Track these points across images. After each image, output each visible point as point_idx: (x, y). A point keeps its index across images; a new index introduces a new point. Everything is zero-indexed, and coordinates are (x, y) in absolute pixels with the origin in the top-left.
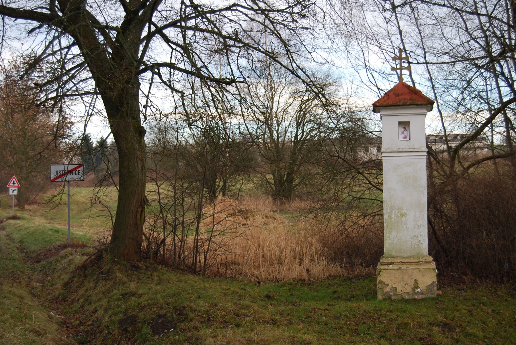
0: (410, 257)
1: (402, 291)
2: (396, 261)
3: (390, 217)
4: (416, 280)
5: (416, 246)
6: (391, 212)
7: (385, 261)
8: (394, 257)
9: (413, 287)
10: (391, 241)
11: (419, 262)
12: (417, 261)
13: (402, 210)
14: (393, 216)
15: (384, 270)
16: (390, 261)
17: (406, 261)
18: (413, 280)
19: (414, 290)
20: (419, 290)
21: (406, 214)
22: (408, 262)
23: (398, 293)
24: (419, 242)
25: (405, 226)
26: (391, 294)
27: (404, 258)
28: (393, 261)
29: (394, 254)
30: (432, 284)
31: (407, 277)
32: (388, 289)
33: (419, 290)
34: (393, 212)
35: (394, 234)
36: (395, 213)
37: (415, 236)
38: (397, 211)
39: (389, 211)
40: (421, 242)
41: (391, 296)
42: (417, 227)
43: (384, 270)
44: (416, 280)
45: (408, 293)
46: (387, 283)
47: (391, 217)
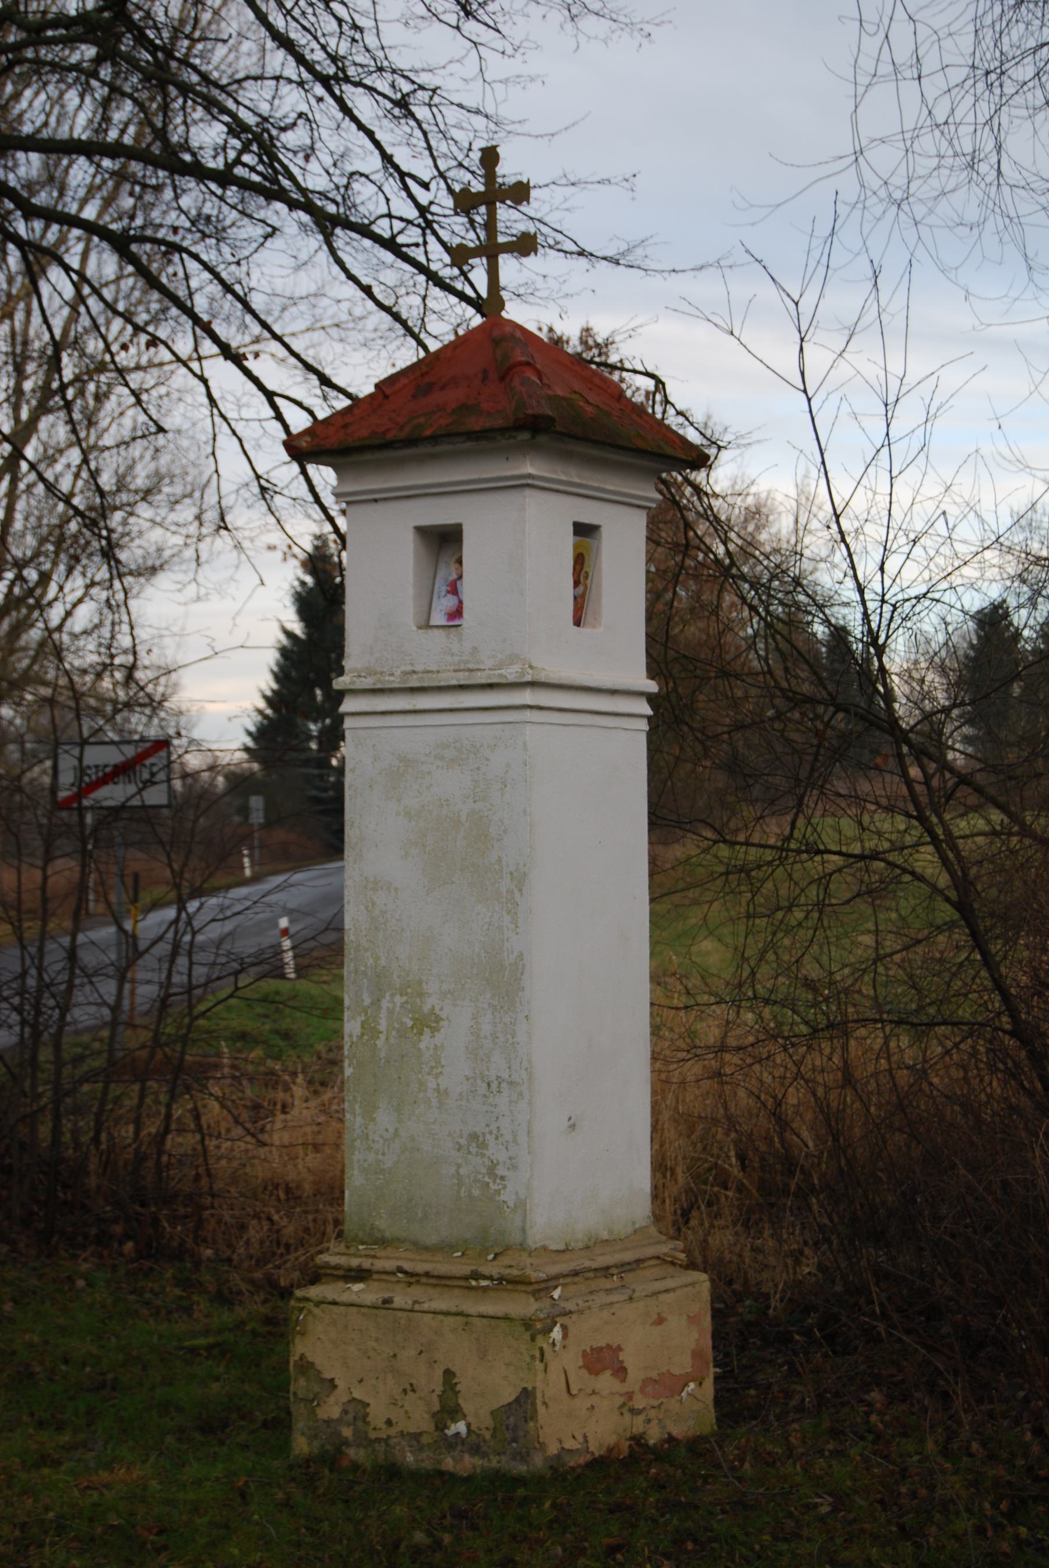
0: (444, 1248)
1: (389, 1422)
2: (379, 1265)
3: (370, 1030)
4: (449, 1374)
5: (476, 1192)
6: (376, 1002)
7: (342, 1260)
8: (384, 1242)
9: (436, 1407)
10: (371, 1157)
11: (476, 1276)
12: (466, 1270)
13: (421, 994)
14: (383, 1025)
15: (318, 1304)
16: (355, 1262)
17: (420, 1268)
18: (439, 1373)
19: (441, 1427)
20: (461, 1427)
21: (438, 1019)
22: (427, 1274)
23: (373, 1435)
24: (491, 1171)
25: (431, 1084)
26: (347, 1432)
27: (426, 1248)
28: (366, 1264)
29: (383, 1224)
30: (517, 1400)
31: (413, 1353)
32: (331, 1409)
33: (461, 1427)
34: (385, 1004)
35: (384, 1118)
36: (390, 1012)
37: (474, 1137)
38: (399, 1000)
39: (367, 1001)
40: (500, 1171)
41: (346, 1443)
42: (482, 1088)
43: (318, 1304)
44: (449, 1374)
45: (417, 1436)
46: (327, 1375)
47: (375, 1033)
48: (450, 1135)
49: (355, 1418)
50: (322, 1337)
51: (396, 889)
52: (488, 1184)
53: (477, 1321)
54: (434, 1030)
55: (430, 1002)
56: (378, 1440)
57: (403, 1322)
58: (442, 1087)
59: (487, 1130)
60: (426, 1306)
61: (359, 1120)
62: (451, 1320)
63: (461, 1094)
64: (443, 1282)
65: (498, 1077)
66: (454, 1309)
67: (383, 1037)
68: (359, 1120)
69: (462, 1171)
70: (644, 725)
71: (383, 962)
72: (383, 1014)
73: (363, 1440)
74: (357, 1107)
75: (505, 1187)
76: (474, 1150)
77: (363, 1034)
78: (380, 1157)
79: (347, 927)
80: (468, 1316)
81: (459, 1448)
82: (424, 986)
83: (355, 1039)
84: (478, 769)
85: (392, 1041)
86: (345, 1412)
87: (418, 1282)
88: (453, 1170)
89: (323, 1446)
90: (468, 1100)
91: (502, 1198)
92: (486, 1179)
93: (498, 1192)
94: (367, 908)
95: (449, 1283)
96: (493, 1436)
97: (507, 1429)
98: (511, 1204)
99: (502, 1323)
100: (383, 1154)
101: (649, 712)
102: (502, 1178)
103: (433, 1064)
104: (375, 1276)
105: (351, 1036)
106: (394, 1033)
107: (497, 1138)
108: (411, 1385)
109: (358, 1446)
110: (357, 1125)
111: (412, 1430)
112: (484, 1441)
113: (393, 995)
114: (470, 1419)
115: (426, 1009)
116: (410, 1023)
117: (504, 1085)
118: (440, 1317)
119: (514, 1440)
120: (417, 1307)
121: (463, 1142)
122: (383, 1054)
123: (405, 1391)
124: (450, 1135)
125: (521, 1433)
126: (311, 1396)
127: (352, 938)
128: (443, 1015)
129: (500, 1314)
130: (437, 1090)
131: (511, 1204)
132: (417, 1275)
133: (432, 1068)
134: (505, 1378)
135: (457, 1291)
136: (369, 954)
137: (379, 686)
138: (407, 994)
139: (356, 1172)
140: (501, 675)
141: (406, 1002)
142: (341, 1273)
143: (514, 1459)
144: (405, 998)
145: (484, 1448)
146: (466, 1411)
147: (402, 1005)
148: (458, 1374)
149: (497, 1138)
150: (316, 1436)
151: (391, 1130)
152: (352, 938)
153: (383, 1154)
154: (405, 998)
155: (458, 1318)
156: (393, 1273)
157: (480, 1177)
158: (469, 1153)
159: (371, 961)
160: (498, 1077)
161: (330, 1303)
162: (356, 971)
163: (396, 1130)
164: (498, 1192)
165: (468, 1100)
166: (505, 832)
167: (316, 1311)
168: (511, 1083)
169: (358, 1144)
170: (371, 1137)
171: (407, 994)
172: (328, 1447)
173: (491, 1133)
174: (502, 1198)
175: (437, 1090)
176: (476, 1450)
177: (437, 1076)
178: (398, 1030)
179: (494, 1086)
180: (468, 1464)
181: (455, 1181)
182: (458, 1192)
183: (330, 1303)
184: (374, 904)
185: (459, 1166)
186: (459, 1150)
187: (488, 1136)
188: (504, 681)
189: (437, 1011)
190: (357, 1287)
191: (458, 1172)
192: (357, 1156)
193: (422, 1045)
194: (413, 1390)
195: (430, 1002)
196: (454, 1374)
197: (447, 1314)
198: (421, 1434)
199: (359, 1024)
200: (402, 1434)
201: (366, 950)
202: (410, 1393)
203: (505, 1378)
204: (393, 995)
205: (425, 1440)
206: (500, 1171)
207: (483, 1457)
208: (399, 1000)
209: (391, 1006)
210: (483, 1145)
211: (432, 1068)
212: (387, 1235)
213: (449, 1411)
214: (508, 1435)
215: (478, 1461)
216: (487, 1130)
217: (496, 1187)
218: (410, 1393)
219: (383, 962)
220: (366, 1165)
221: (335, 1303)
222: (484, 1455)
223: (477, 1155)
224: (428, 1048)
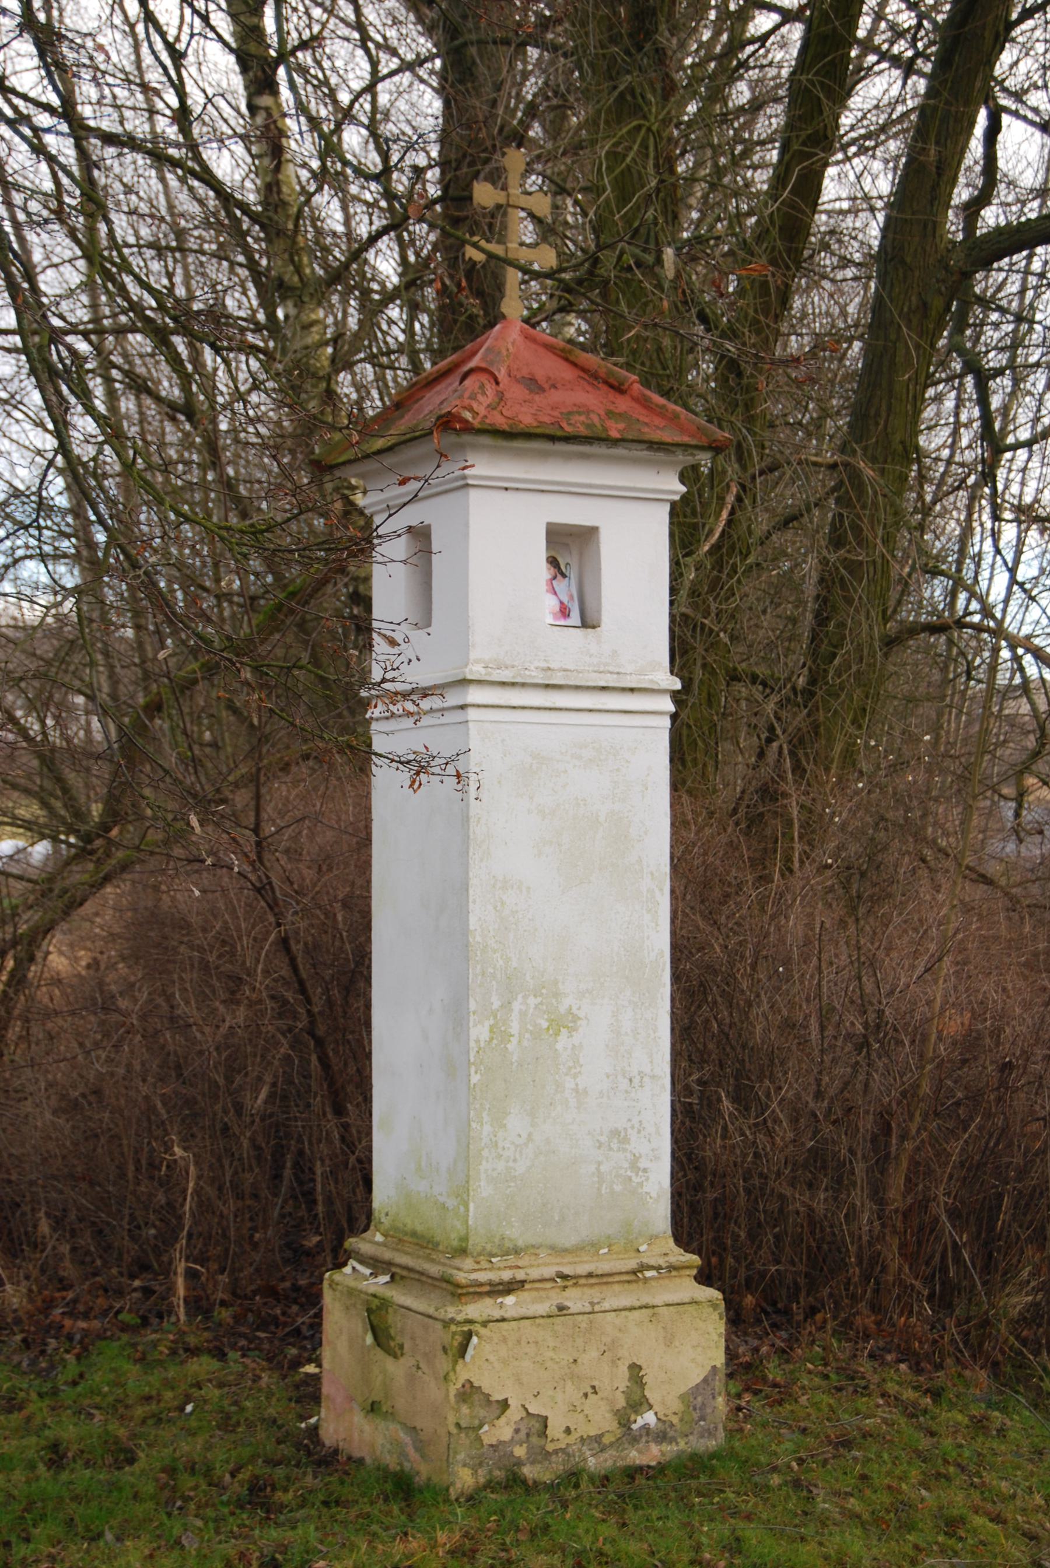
0: (592, 1247)
1: (568, 1431)
2: (535, 1273)
3: (499, 1034)
4: (635, 1369)
5: (618, 1188)
6: (507, 1005)
8: (517, 1251)
9: (621, 1402)
10: (501, 1166)
11: (643, 1267)
12: (632, 1264)
13: (557, 995)
14: (515, 1027)
15: (485, 1324)
16: (506, 1275)
17: (582, 1269)
18: (623, 1371)
19: (625, 1423)
20: (649, 1418)
21: (576, 1018)
22: (590, 1275)
23: (550, 1447)
24: (634, 1165)
25: (569, 1083)
26: (520, 1451)
27: (566, 1251)
28: (520, 1275)
29: (516, 1233)
30: (705, 1380)
31: (594, 1354)
32: (502, 1431)
33: (649, 1418)
34: (516, 1006)
35: (516, 1123)
36: (523, 1014)
37: (615, 1133)
38: (532, 1001)
39: (496, 1004)
40: (642, 1164)
41: (519, 1463)
42: (624, 1084)
43: (485, 1324)
44: (635, 1369)
45: (598, 1438)
46: (497, 1396)
47: (506, 1037)
48: (589, 1133)
49: (528, 1435)
50: (492, 1358)
51: (528, 888)
52: (630, 1179)
53: (664, 1310)
54: (572, 1030)
55: (567, 1002)
56: (556, 1452)
57: (583, 1325)
58: (580, 1087)
59: (629, 1124)
60: (606, 1305)
61: (487, 1129)
62: (636, 1314)
63: (601, 1092)
64: (605, 1280)
65: (640, 1073)
66: (638, 1304)
67: (514, 1041)
68: (487, 1129)
69: (602, 1168)
70: (667, 722)
71: (514, 964)
72: (515, 1016)
73: (543, 1455)
74: (485, 1114)
75: (647, 1179)
76: (615, 1146)
77: (492, 1039)
78: (511, 1164)
79: (472, 927)
80: (654, 1307)
81: (644, 1439)
82: (560, 986)
83: (482, 1044)
84: (618, 770)
85: (525, 1043)
86: (517, 1431)
87: (575, 1284)
88: (593, 1168)
89: (490, 1472)
90: (609, 1098)
91: (645, 1189)
92: (629, 1173)
93: (641, 1184)
94: (495, 908)
95: (610, 1279)
96: (681, 1420)
97: (695, 1409)
98: (654, 1194)
99: (690, 1308)
100: (515, 1161)
101: (672, 708)
102: (645, 1170)
103: (571, 1064)
104: (527, 1286)
105: (477, 1041)
106: (527, 1035)
107: (639, 1132)
108: (593, 1387)
109: (533, 1463)
110: (485, 1133)
111: (593, 1433)
112: (672, 1425)
113: (525, 997)
114: (656, 1408)
115: (562, 1009)
116: (545, 1025)
117: (646, 1079)
118: (623, 1313)
119: (702, 1418)
120: (597, 1308)
121: (603, 1139)
122: (515, 1058)
123: (586, 1395)
124: (589, 1133)
125: (709, 1410)
126: (476, 1422)
127: (478, 939)
128: (581, 1014)
129: (687, 1300)
130: (576, 1090)
131: (654, 1194)
132: (580, 1277)
133: (570, 1068)
134: (693, 1360)
135: (616, 1287)
136: (498, 955)
137: (519, 680)
138: (541, 995)
139: (482, 1183)
140: (652, 681)
141: (541, 1003)
142: (487, 1288)
143: (702, 1437)
144: (539, 999)
145: (671, 1433)
146: (651, 1401)
147: (536, 1007)
148: (644, 1366)
149: (639, 1132)
150: (481, 1464)
151: (524, 1135)
152: (478, 939)
153: (515, 1161)
154: (539, 999)
155: (644, 1311)
156: (553, 1280)
157: (622, 1172)
158: (611, 1149)
159: (501, 962)
160: (640, 1073)
161: (497, 1321)
162: (483, 974)
163: (530, 1135)
164: (641, 1184)
165: (609, 1098)
166: (646, 833)
167: (483, 1331)
168: (653, 1077)
169: (485, 1153)
170: (501, 1144)
171: (541, 995)
172: (497, 1473)
173: (633, 1127)
174: (645, 1189)
175: (576, 1090)
176: (662, 1437)
177: (575, 1076)
178: (531, 1033)
179: (636, 1081)
180: (653, 1454)
181: (596, 1179)
182: (599, 1189)
183: (497, 1321)
184: (503, 903)
185: (599, 1163)
186: (599, 1147)
187: (630, 1131)
188: (656, 687)
189: (574, 1010)
190: (510, 1300)
191: (598, 1169)
192: (484, 1166)
193: (559, 1046)
194: (596, 1393)
195: (567, 1002)
196: (640, 1368)
197: (632, 1309)
198: (602, 1435)
199: (487, 1027)
200: (582, 1439)
201: (495, 951)
202: (591, 1396)
203: (693, 1360)
204: (525, 997)
205: (606, 1440)
206: (642, 1164)
207: (670, 1443)
208: (532, 1001)
209: (523, 1008)
210: (626, 1140)
211: (570, 1068)
212: (520, 1243)
213: (638, 1403)
214: (696, 1415)
215: (666, 1448)
216: (629, 1124)
217: (638, 1180)
218: (591, 1396)
219: (514, 964)
220: (495, 1174)
221: (503, 1320)
222: (673, 1440)
223: (619, 1150)
224: (565, 1049)
